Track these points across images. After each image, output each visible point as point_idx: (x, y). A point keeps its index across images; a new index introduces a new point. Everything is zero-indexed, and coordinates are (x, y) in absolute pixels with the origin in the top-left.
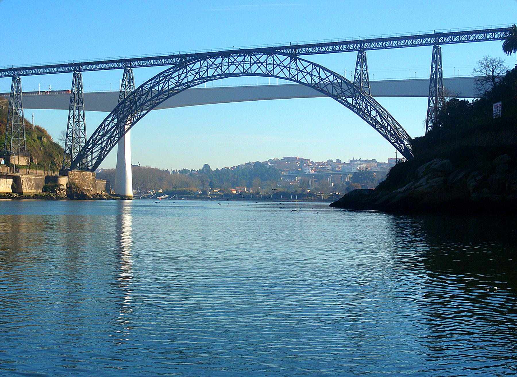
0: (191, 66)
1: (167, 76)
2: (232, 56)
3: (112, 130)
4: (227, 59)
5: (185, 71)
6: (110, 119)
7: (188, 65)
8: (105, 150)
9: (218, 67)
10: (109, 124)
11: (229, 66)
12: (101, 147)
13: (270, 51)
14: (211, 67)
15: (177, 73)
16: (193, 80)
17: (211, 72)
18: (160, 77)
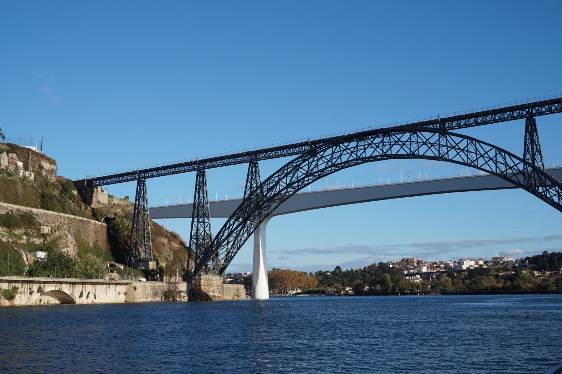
0: (321, 154)
1: (297, 166)
3: (239, 229)
7: (318, 153)
8: (231, 252)
10: (234, 223)
11: (365, 149)
14: (345, 152)
16: (326, 168)
17: (344, 158)
18: (288, 168)
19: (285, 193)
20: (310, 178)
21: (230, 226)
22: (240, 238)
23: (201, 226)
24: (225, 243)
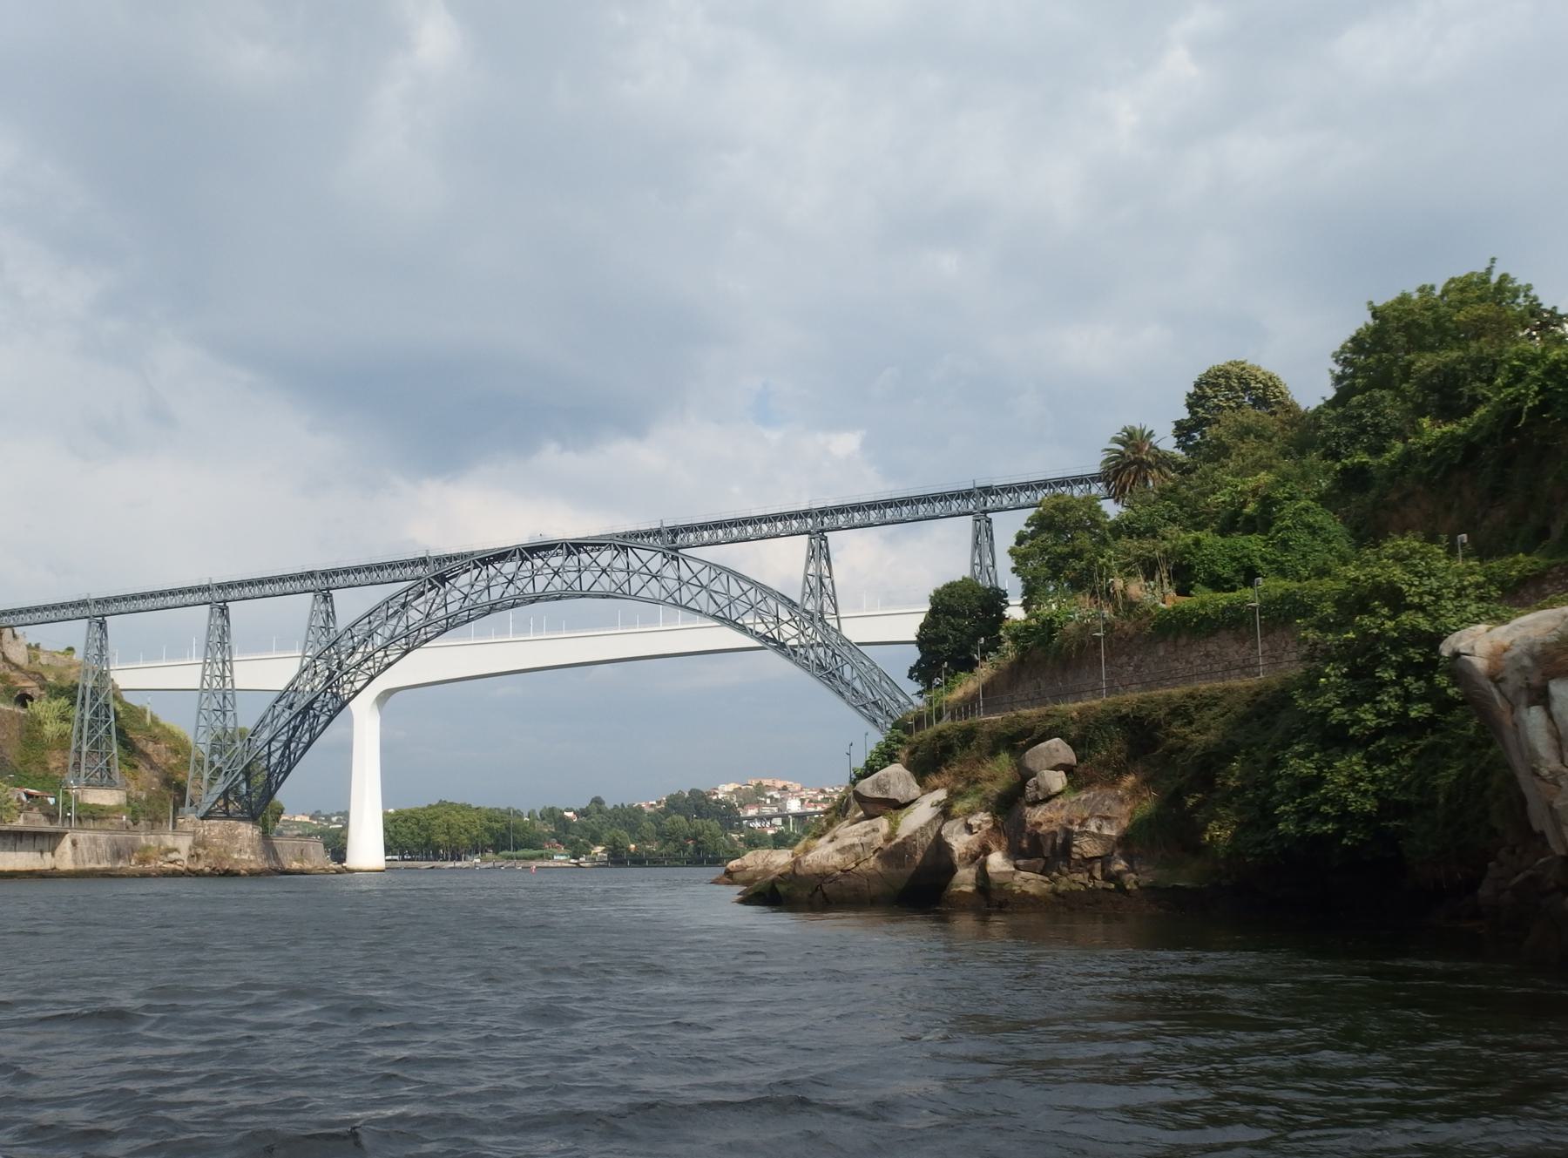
1: (404, 606)
2: (540, 557)
9: (511, 582)
12: (268, 768)
17: (496, 593)
20: (428, 629)
22: (293, 745)
23: (217, 718)
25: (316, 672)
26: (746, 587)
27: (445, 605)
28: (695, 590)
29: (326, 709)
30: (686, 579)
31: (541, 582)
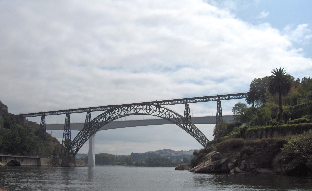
0: (115, 111)
1: (105, 115)
2: (132, 106)
3: (82, 138)
4: (130, 108)
5: (112, 113)
6: (81, 133)
9: (126, 111)
11: (131, 110)
12: (77, 146)
13: (148, 104)
14: (123, 111)
15: (109, 114)
16: (116, 116)
17: (123, 113)
18: (102, 116)
19: (100, 125)
21: (78, 137)
24: (76, 143)
25: (87, 127)
26: (173, 113)
27: (113, 115)
28: (163, 114)
29: (89, 135)
30: (161, 111)
31: (132, 111)
